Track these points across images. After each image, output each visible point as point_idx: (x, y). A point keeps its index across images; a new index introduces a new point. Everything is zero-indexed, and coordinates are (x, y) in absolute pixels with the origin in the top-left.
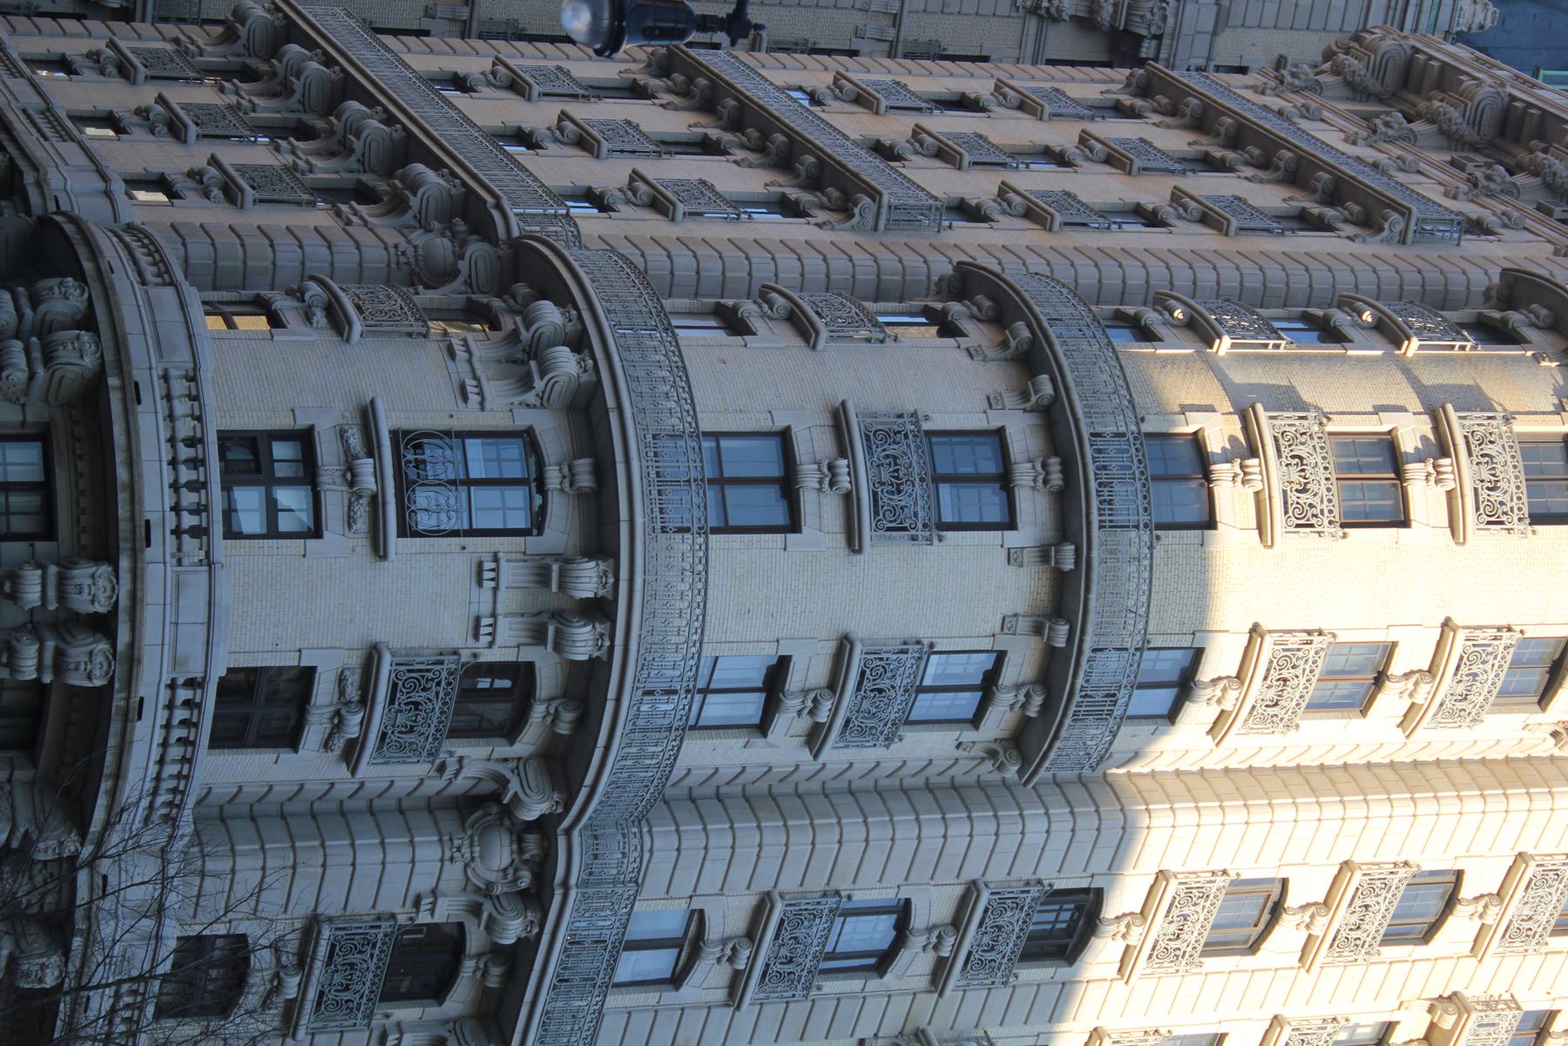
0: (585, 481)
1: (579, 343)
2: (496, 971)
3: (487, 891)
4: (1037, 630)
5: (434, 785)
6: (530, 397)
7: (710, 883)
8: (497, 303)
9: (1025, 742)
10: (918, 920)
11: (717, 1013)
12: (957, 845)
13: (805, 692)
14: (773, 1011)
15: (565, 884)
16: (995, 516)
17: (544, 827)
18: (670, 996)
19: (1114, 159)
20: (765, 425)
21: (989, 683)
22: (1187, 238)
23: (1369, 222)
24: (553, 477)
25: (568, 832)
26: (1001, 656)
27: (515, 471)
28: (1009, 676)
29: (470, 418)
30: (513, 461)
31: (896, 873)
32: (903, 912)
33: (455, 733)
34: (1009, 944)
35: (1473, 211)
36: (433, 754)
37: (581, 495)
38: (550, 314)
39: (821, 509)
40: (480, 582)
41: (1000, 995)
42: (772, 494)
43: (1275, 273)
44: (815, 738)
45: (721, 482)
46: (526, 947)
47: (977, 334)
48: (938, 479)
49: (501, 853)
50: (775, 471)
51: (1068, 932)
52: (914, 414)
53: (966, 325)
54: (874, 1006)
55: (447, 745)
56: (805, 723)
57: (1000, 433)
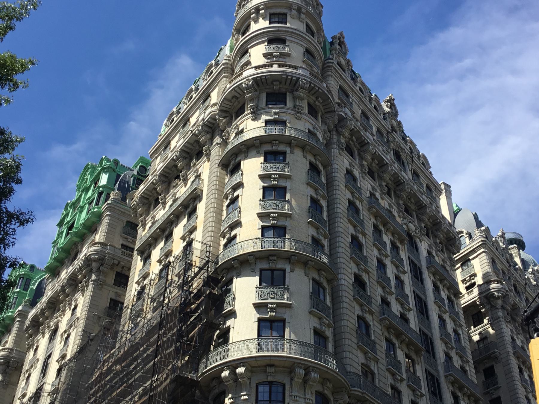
7: (357, 360)
12: (347, 300)
13: (321, 324)
15: (363, 393)
22: (198, 236)
24: (270, 379)
25: (351, 390)
27: (267, 388)
28: (317, 278)
31: (353, 316)
38: (225, 374)
40: (297, 401)
44: (329, 326)
52: (256, 288)
54: (376, 329)
57: (261, 271)
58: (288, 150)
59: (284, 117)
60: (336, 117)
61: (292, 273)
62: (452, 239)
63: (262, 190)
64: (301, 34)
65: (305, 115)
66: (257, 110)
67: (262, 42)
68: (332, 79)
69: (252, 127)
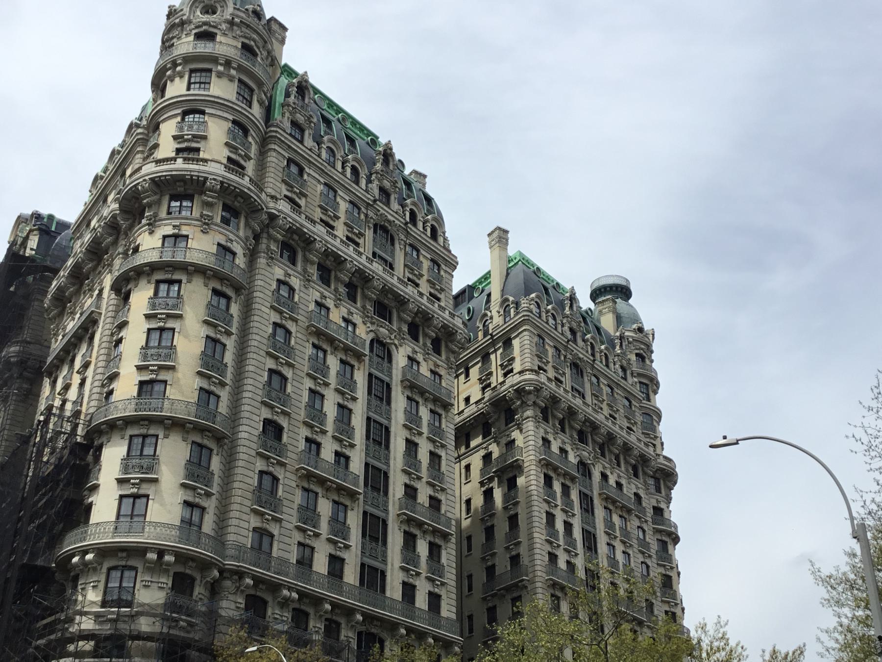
0: (124, 554)
1: (86, 552)
2: (261, 586)
3: (238, 588)
4: (188, 432)
5: (206, 601)
6: (99, 568)
7: (246, 525)
8: (72, 574)
9: (219, 438)
10: (265, 468)
11: (283, 525)
13: (195, 497)
14: (285, 509)
16: (154, 440)
17: (221, 572)
18: (276, 538)
19: (67, 387)
20: (116, 503)
21: (201, 446)
22: (90, 372)
23: (95, 322)
24: (124, 563)
26: (193, 442)
27: (119, 574)
29: (101, 586)
30: (116, 574)
32: (261, 473)
33: (191, 595)
34: (276, 444)
35: (97, 292)
36: (196, 601)
37: (128, 557)
38: (75, 559)
39: (145, 489)
41: (290, 447)
42: (138, 501)
43: (103, 351)
45: (132, 516)
46: (254, 578)
47: (104, 439)
48: (141, 455)
49: (228, 583)
50: (131, 500)
51: (275, 428)
53: (100, 441)
55: (194, 597)
56: (204, 498)
57: (131, 436)
58: (184, 279)
59: (185, 231)
60: (265, 217)
61: (166, 440)
62: (453, 334)
63: (145, 335)
64: (226, 103)
65: (216, 225)
66: (155, 221)
67: (175, 116)
68: (274, 154)
69: (149, 244)
